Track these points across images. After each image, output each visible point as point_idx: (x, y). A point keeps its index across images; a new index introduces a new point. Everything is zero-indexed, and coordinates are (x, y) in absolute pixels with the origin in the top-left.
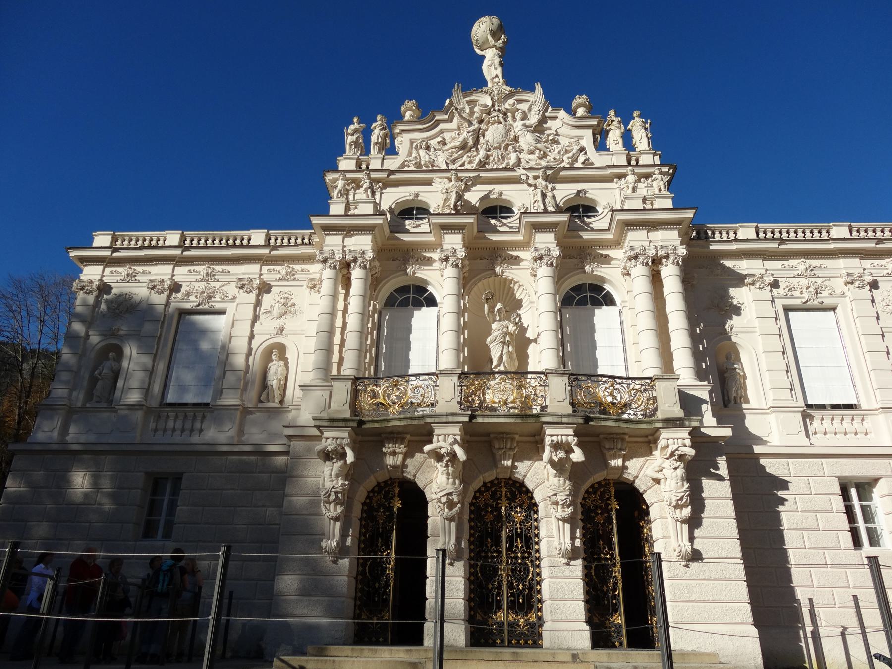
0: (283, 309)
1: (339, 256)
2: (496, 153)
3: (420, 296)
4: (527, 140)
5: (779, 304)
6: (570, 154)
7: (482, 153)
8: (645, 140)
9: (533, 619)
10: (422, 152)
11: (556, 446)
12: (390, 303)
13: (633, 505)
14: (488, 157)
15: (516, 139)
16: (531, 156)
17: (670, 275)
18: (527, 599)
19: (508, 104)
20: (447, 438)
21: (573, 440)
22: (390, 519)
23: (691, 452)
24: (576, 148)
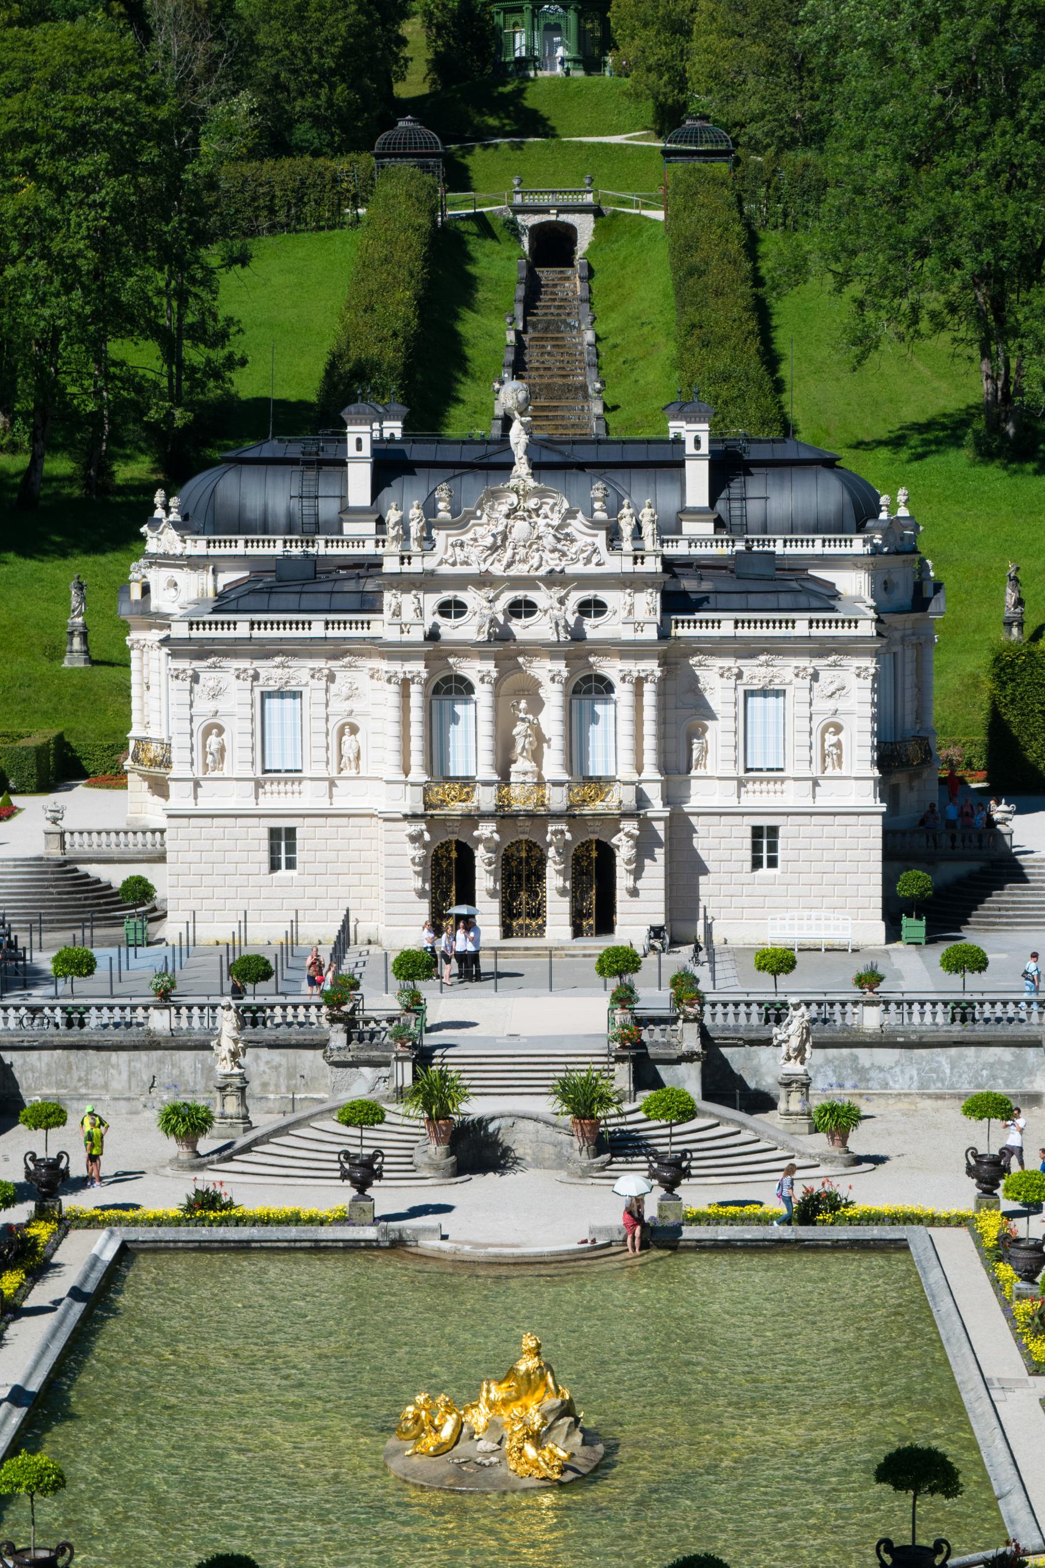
0: (350, 693)
1: (401, 676)
2: (522, 552)
3: (462, 688)
4: (549, 541)
5: (741, 690)
6: (585, 555)
7: (509, 552)
8: (651, 538)
9: (540, 922)
10: (458, 549)
11: (555, 833)
12: (437, 690)
13: (607, 854)
14: (514, 555)
15: (539, 538)
16: (552, 556)
17: (649, 688)
18: (537, 912)
19: (532, 503)
20: (486, 830)
21: (565, 828)
22: (450, 864)
23: (637, 832)
24: (590, 549)
